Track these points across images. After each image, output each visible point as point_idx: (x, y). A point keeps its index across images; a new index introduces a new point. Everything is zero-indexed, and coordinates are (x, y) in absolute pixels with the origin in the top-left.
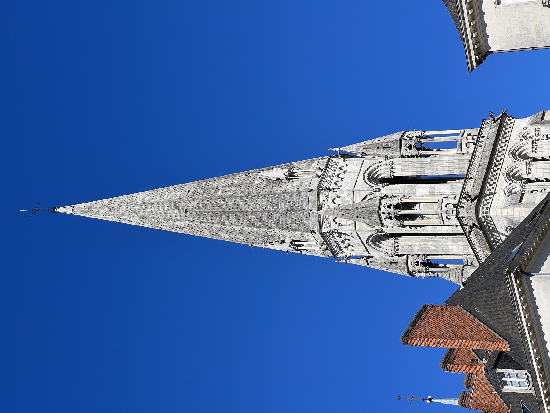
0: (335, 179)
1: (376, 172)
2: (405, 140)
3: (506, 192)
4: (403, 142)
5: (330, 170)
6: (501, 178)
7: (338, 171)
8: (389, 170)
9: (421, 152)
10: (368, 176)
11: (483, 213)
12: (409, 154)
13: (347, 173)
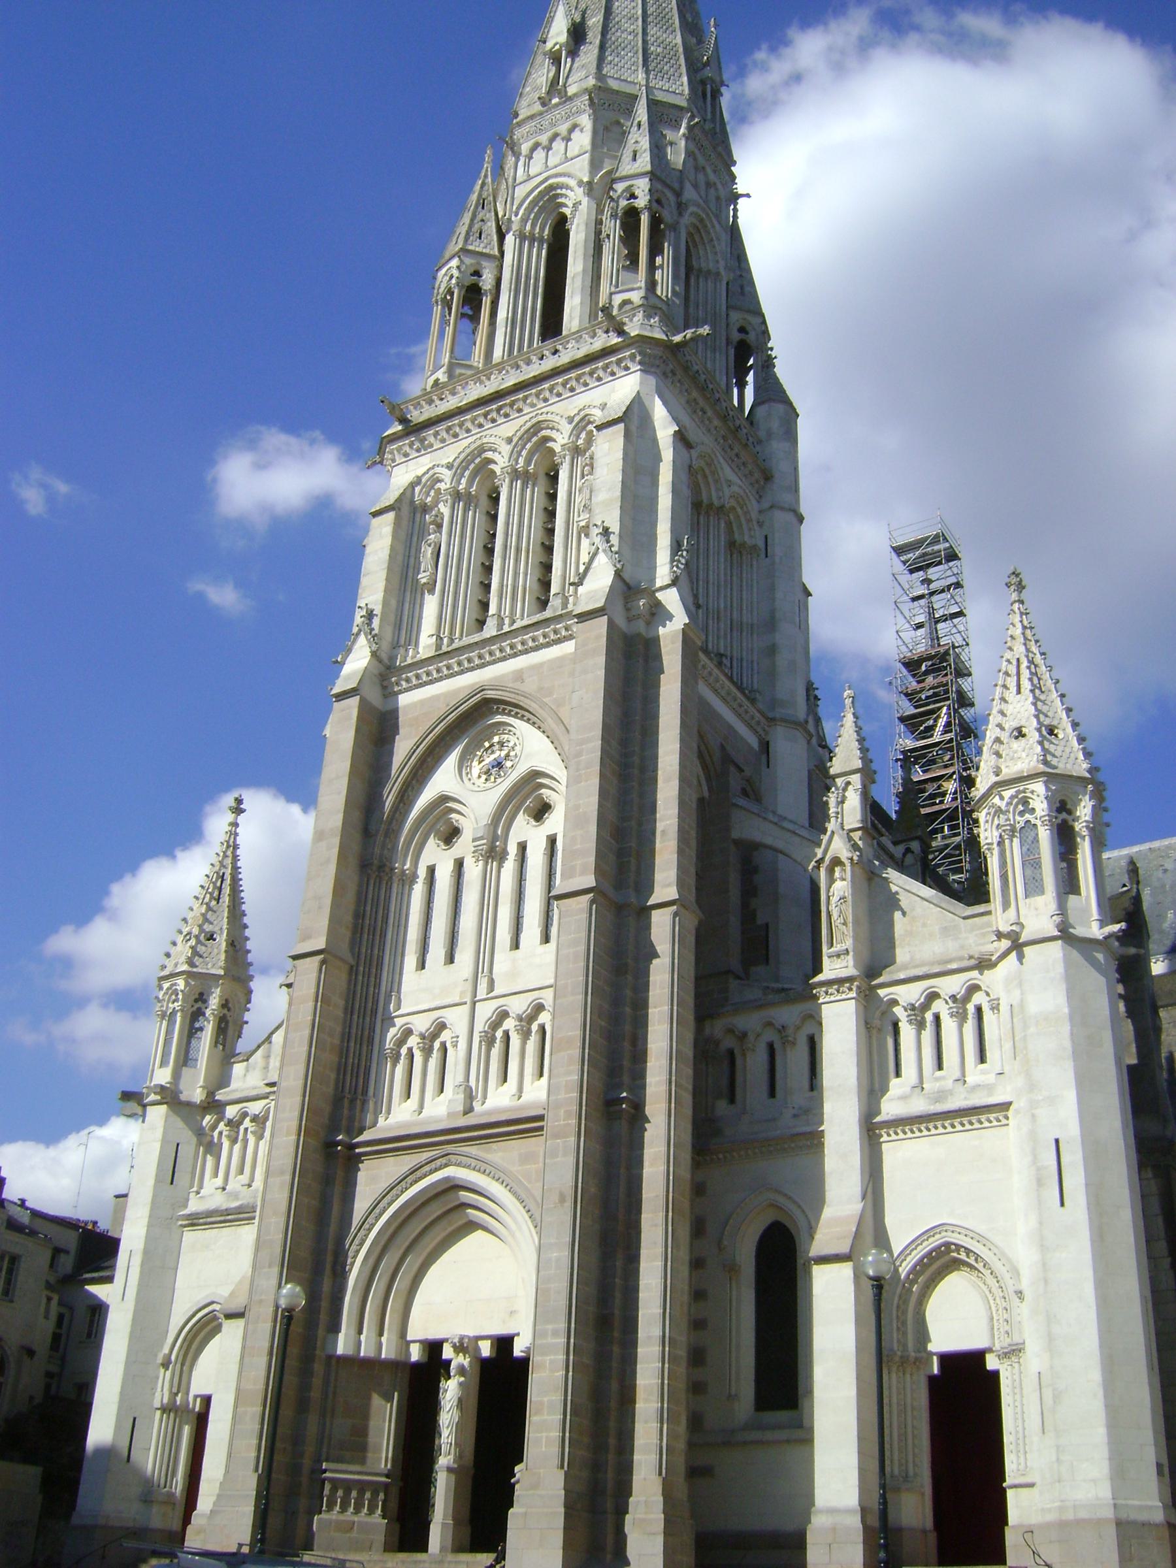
0: (544, 139)
3: (431, 473)
10: (552, 188)
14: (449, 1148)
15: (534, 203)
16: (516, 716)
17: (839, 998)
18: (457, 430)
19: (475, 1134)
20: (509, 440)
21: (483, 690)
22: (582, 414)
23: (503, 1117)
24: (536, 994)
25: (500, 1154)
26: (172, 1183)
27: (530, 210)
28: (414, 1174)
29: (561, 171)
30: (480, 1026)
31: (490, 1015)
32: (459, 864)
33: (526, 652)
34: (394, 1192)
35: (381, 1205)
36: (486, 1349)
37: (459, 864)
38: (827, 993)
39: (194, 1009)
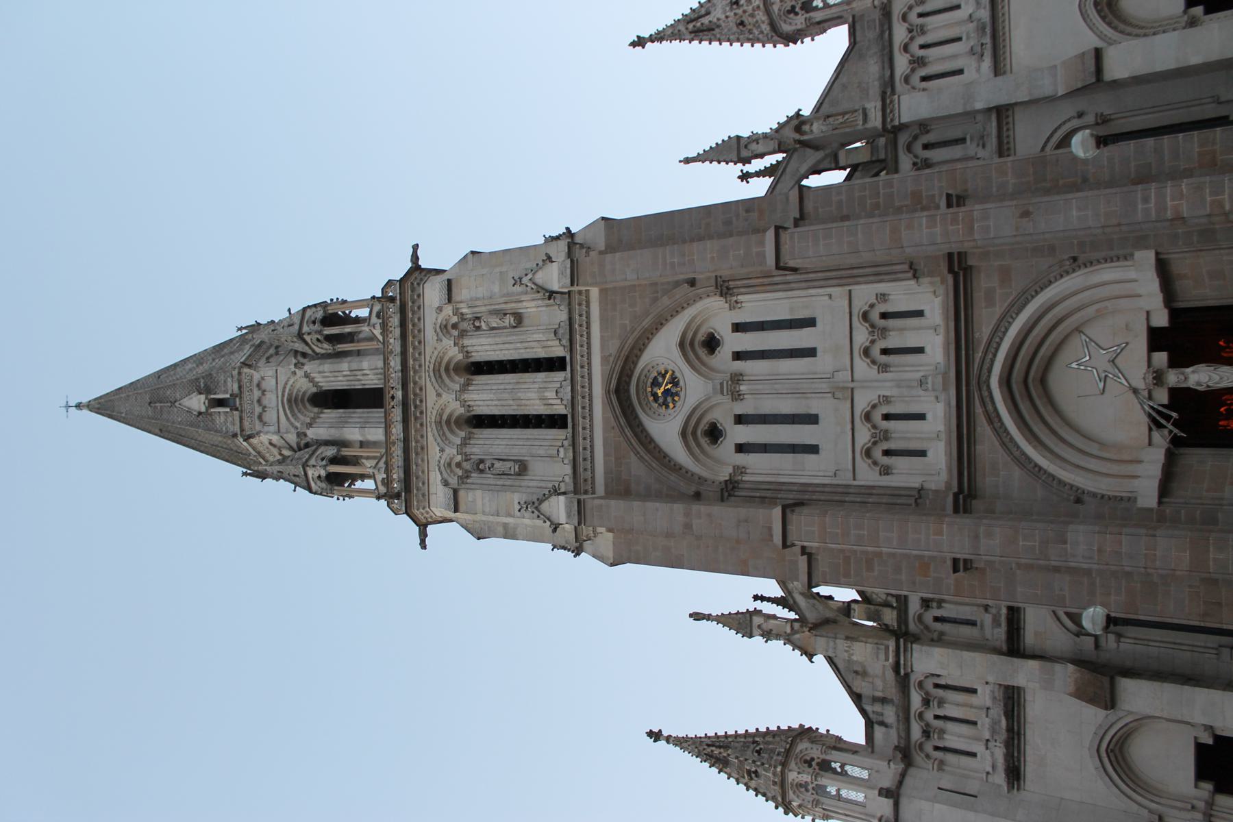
0: (258, 410)
1: (299, 391)
2: (303, 334)
4: (305, 336)
5: (247, 394)
6: (430, 435)
7: (257, 393)
8: (311, 384)
9: (336, 347)
10: (289, 401)
11: (422, 514)
12: (323, 351)
13: (268, 395)
14: (974, 382)
15: (294, 415)
16: (635, 364)
17: (897, 111)
18: (419, 445)
19: (963, 352)
20: (439, 395)
21: (609, 392)
22: (438, 330)
23: (952, 324)
24: (855, 319)
25: (984, 330)
26: (976, 797)
27: (297, 418)
28: (993, 418)
29: (282, 386)
30: (873, 372)
31: (865, 365)
32: (740, 419)
33: (589, 354)
34: (1007, 440)
35: (1017, 454)
36: (1161, 358)
37: (740, 419)
38: (892, 120)
39: (817, 767)
